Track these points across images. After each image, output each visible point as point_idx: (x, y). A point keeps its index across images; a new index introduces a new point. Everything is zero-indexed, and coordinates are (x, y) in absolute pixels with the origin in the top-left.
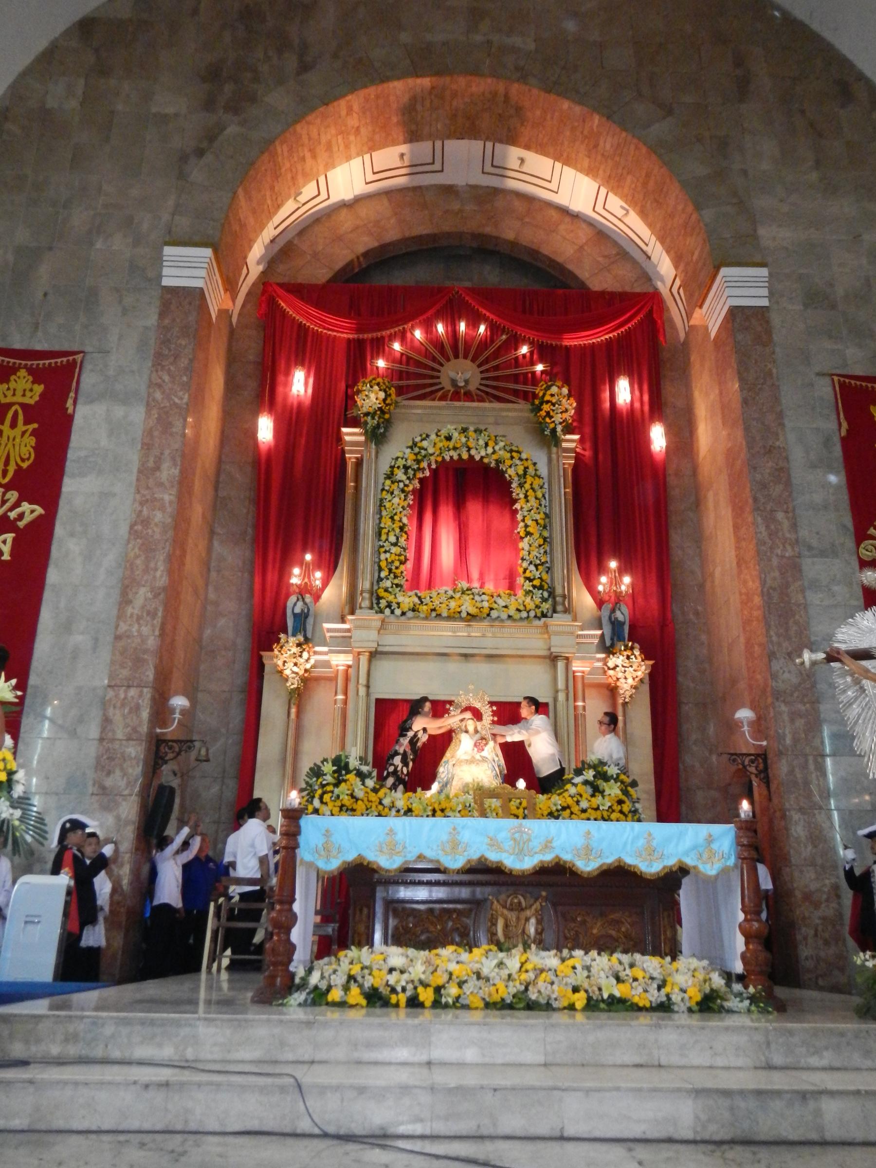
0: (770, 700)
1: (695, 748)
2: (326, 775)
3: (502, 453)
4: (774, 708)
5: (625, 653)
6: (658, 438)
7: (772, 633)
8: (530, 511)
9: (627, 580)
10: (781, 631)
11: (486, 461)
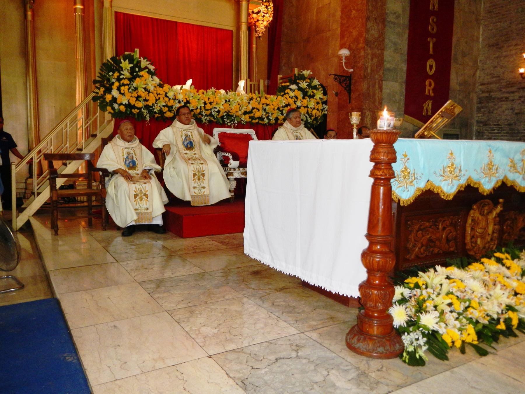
0: (361, 45)
1: (284, 68)
2: (123, 71)
4: (364, 50)
5: (265, 4)
7: (370, 4)
10: (374, 3)
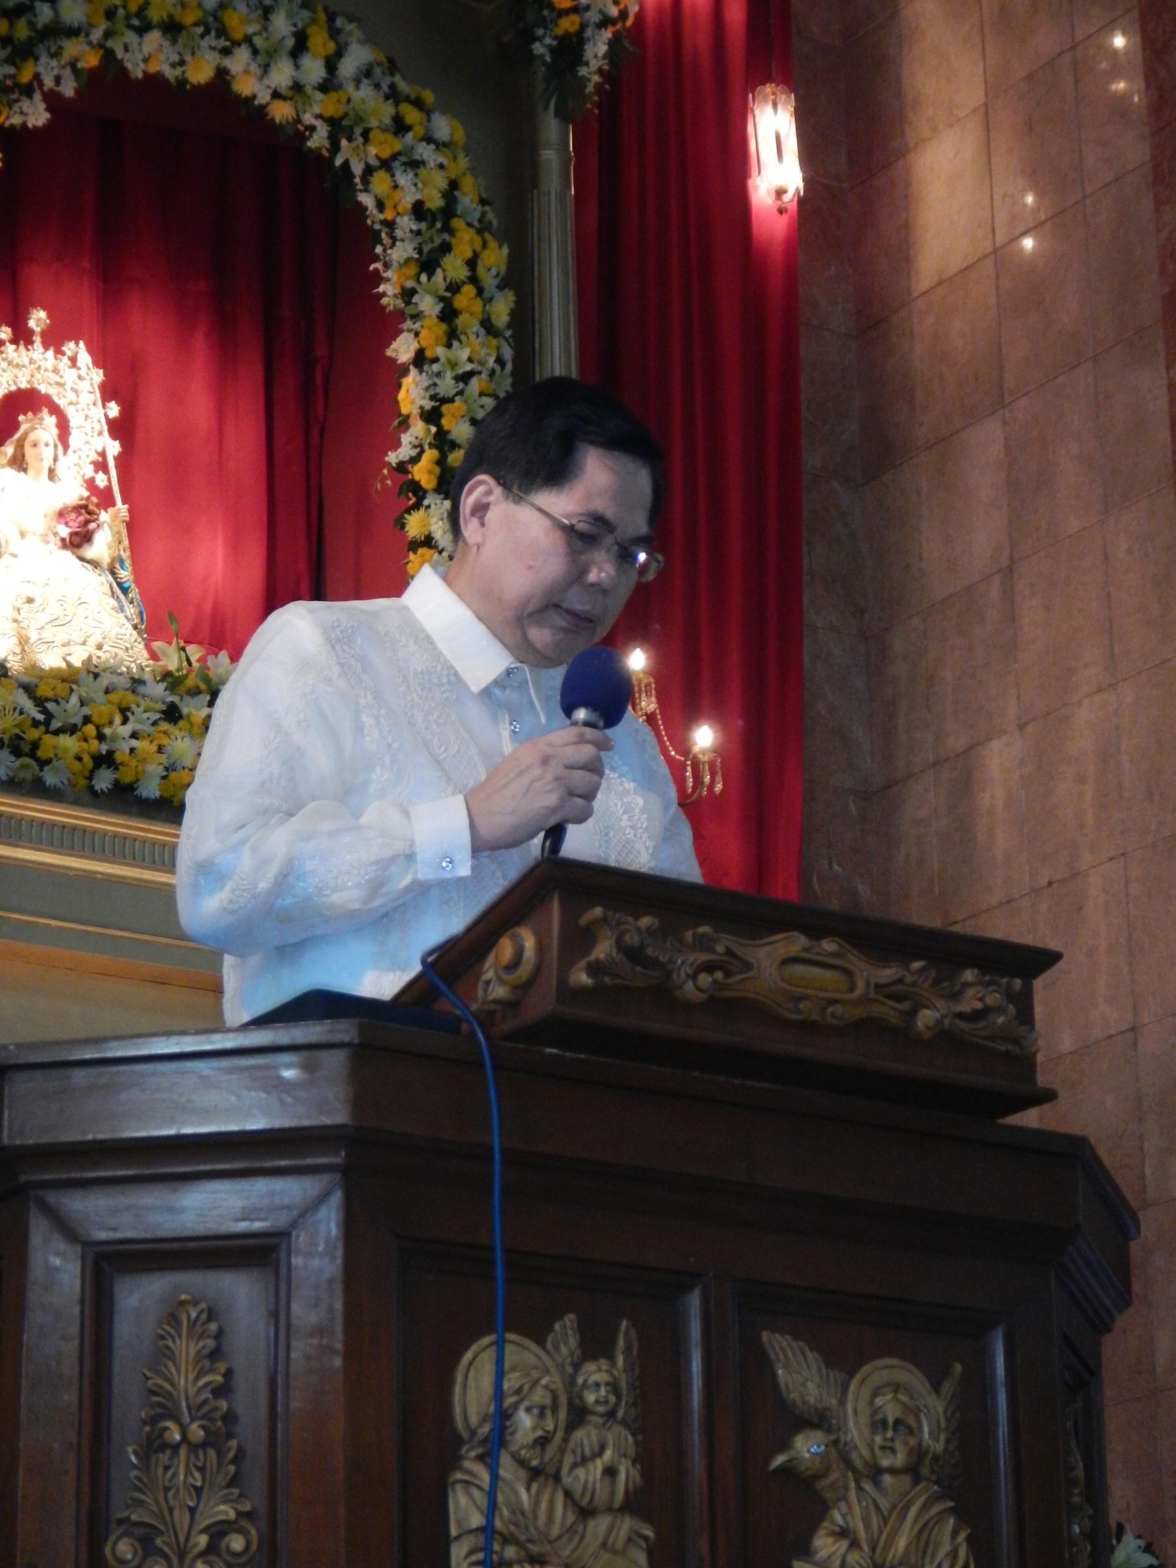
3: (365, 96)
6: (775, 155)
8: (465, 378)
9: (704, 737)
11: (281, 112)
